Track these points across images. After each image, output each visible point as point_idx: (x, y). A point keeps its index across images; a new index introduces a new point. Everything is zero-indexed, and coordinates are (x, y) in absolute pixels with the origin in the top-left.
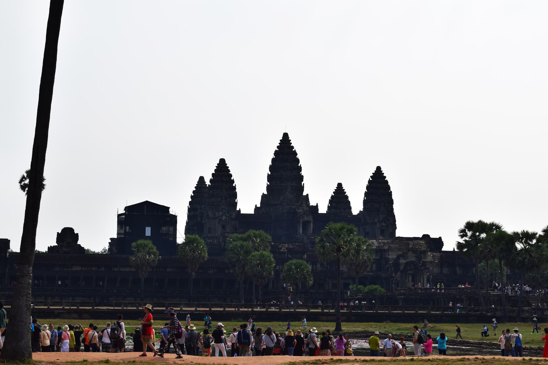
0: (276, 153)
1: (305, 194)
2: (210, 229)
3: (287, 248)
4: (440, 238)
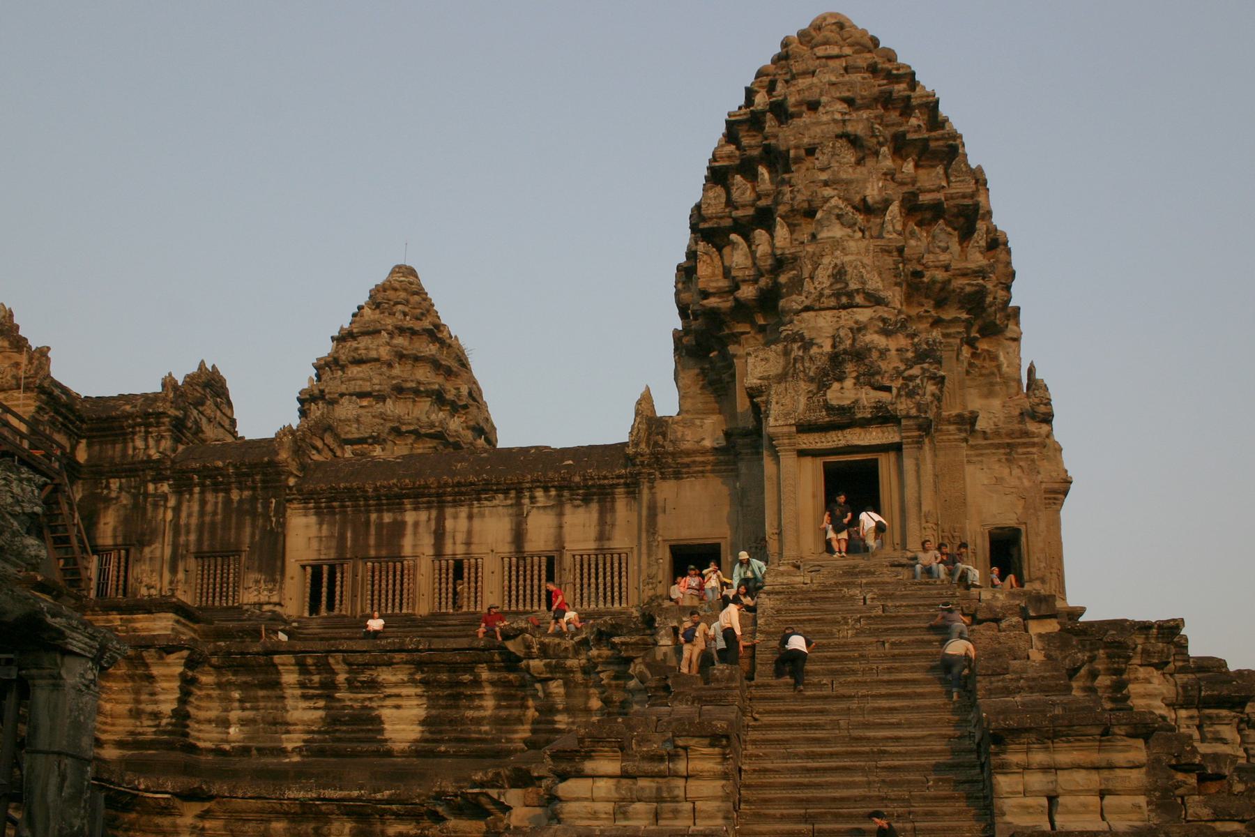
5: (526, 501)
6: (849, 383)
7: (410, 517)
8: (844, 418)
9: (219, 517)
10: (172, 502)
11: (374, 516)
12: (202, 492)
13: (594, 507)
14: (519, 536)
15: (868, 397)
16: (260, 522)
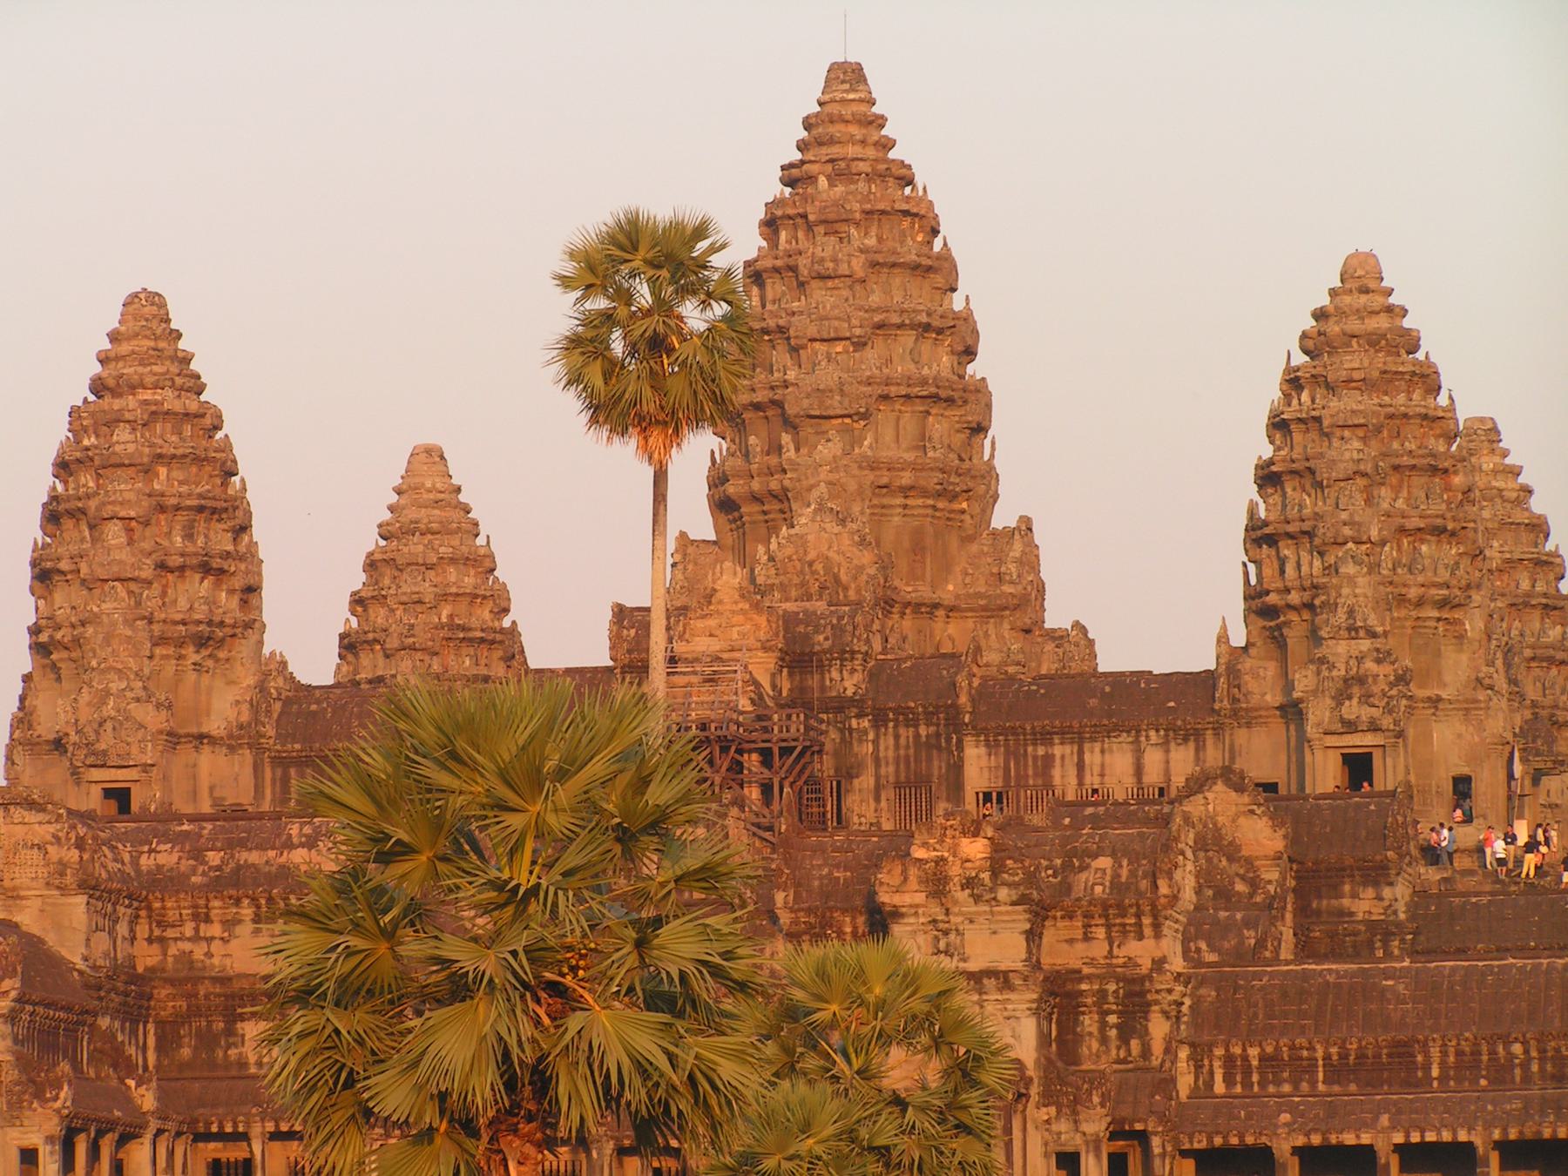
1: (1003, 517)
5: (1143, 739)
6: (1355, 701)
7: (1058, 751)
8: (1350, 727)
9: (912, 751)
10: (871, 736)
11: (1030, 749)
12: (895, 727)
13: (1192, 745)
14: (1139, 771)
15: (1366, 713)
16: (944, 756)
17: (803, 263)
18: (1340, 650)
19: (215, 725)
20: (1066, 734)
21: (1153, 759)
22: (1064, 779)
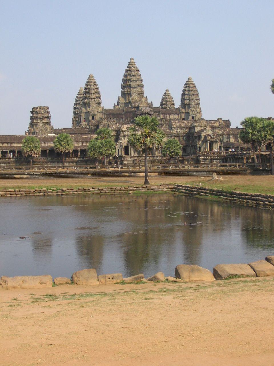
0: (127, 71)
2: (84, 119)
3: (127, 128)
4: (228, 120)
8: (193, 114)
17: (132, 74)
18: (192, 108)
19: (99, 111)
20: (168, 114)
21: (175, 116)
22: (168, 117)
